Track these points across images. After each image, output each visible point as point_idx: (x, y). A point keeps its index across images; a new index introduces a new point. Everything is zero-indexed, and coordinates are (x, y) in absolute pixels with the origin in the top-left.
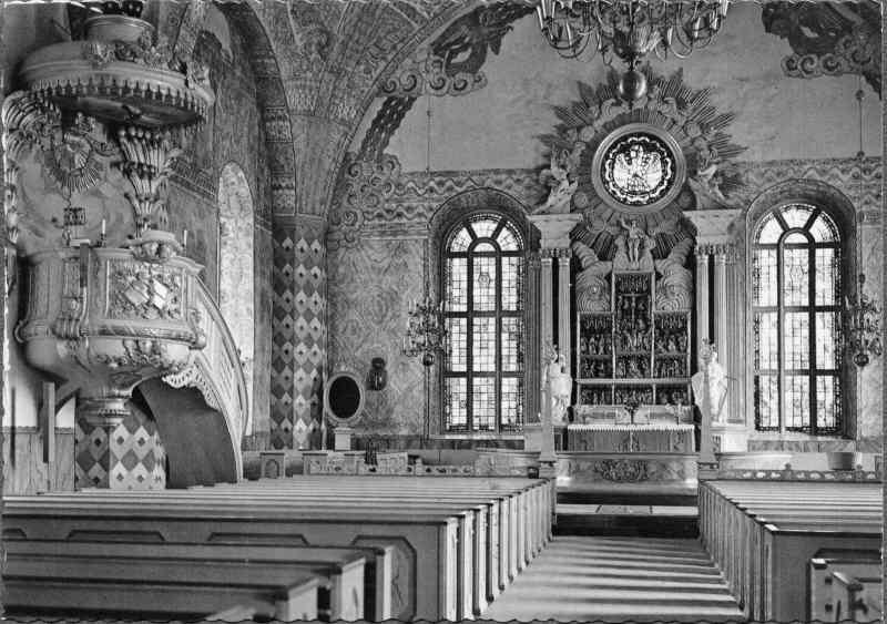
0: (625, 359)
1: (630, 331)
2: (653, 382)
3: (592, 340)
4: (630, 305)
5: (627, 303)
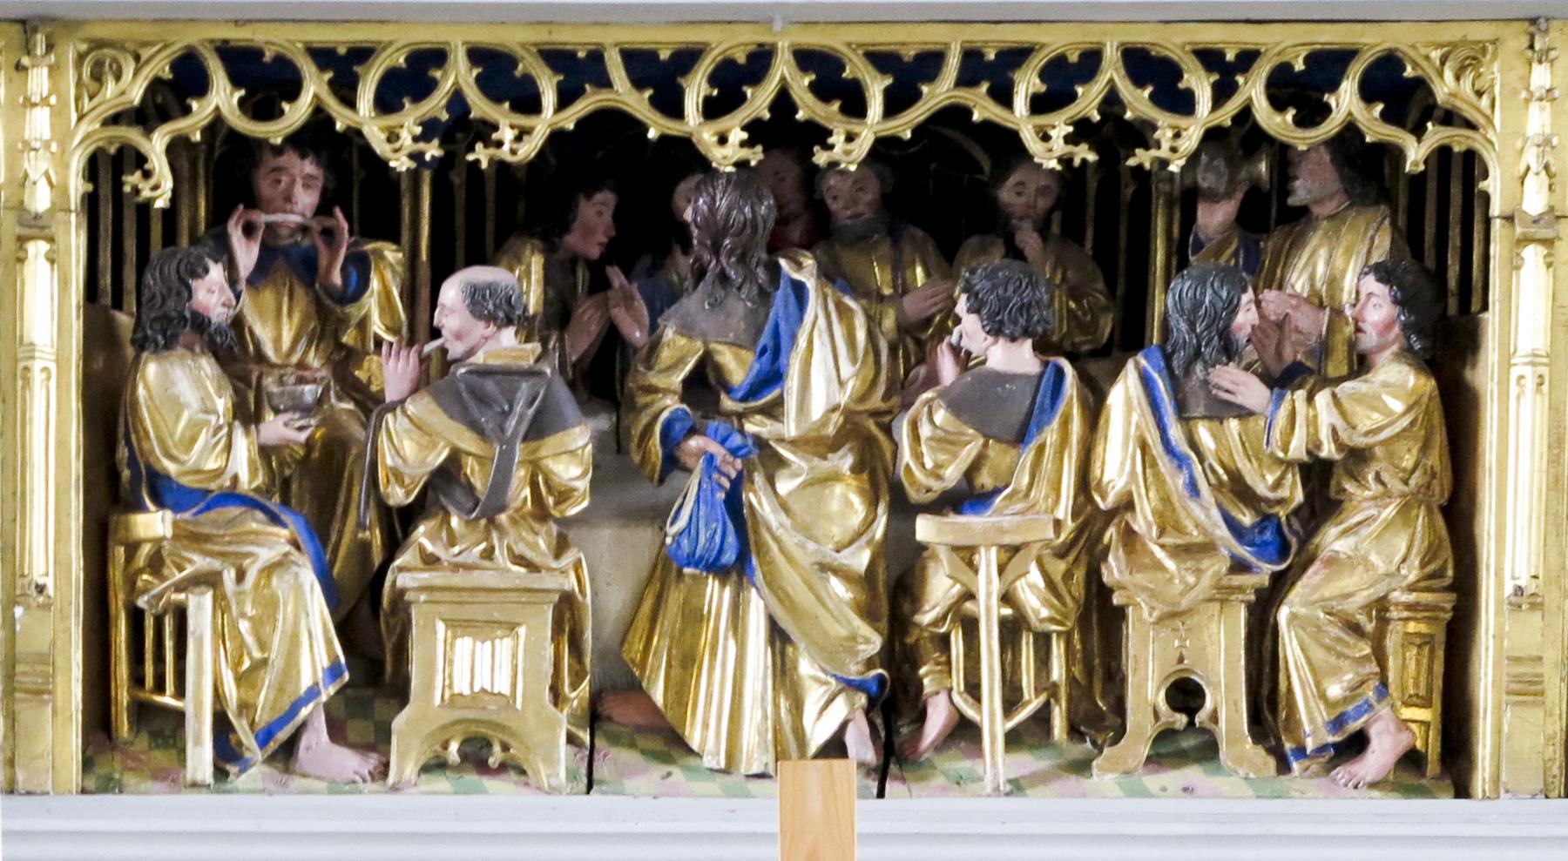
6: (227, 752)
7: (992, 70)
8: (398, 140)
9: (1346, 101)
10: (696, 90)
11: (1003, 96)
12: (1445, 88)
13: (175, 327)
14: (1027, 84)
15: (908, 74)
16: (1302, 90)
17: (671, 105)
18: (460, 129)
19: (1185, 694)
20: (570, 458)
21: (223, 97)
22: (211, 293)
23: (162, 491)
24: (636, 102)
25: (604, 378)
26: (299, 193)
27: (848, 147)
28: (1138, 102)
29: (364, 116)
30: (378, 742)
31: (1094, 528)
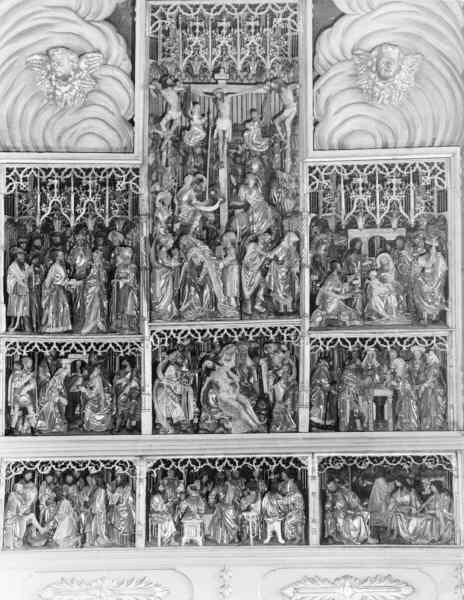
0: (197, 356)
1: (211, 237)
2: (311, 448)
3: (57, 272)
4: (209, 129)
5: (196, 119)
6: (162, 544)
7: (250, 460)
8: (182, 469)
9: (291, 463)
10: (217, 463)
11: (252, 463)
12: (302, 461)
13: (156, 492)
14: (254, 462)
15: (241, 461)
16: (287, 461)
17: (214, 465)
18: (190, 468)
19: (274, 533)
20: (202, 507)
21: (162, 465)
22: (161, 488)
23: (154, 512)
24: (208, 464)
25: (206, 496)
26: (171, 475)
27: (234, 469)
28: (267, 464)
29: (179, 467)
30: (180, 542)
31: (263, 513)
